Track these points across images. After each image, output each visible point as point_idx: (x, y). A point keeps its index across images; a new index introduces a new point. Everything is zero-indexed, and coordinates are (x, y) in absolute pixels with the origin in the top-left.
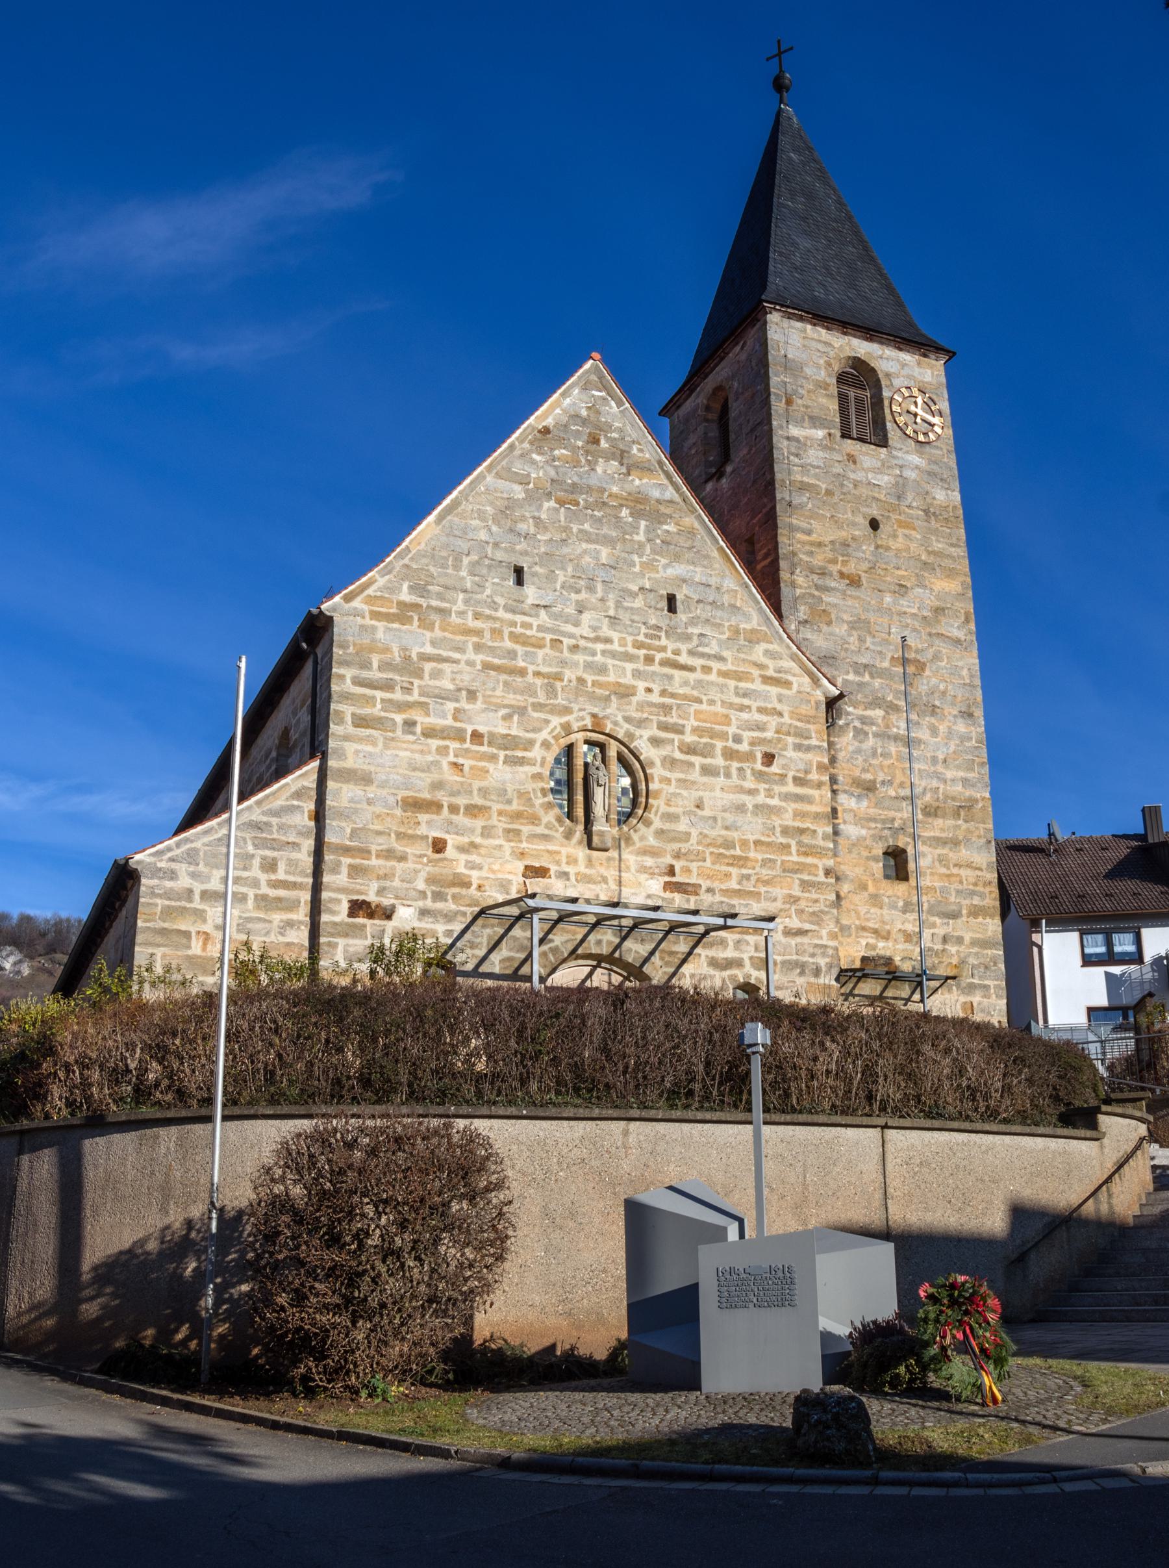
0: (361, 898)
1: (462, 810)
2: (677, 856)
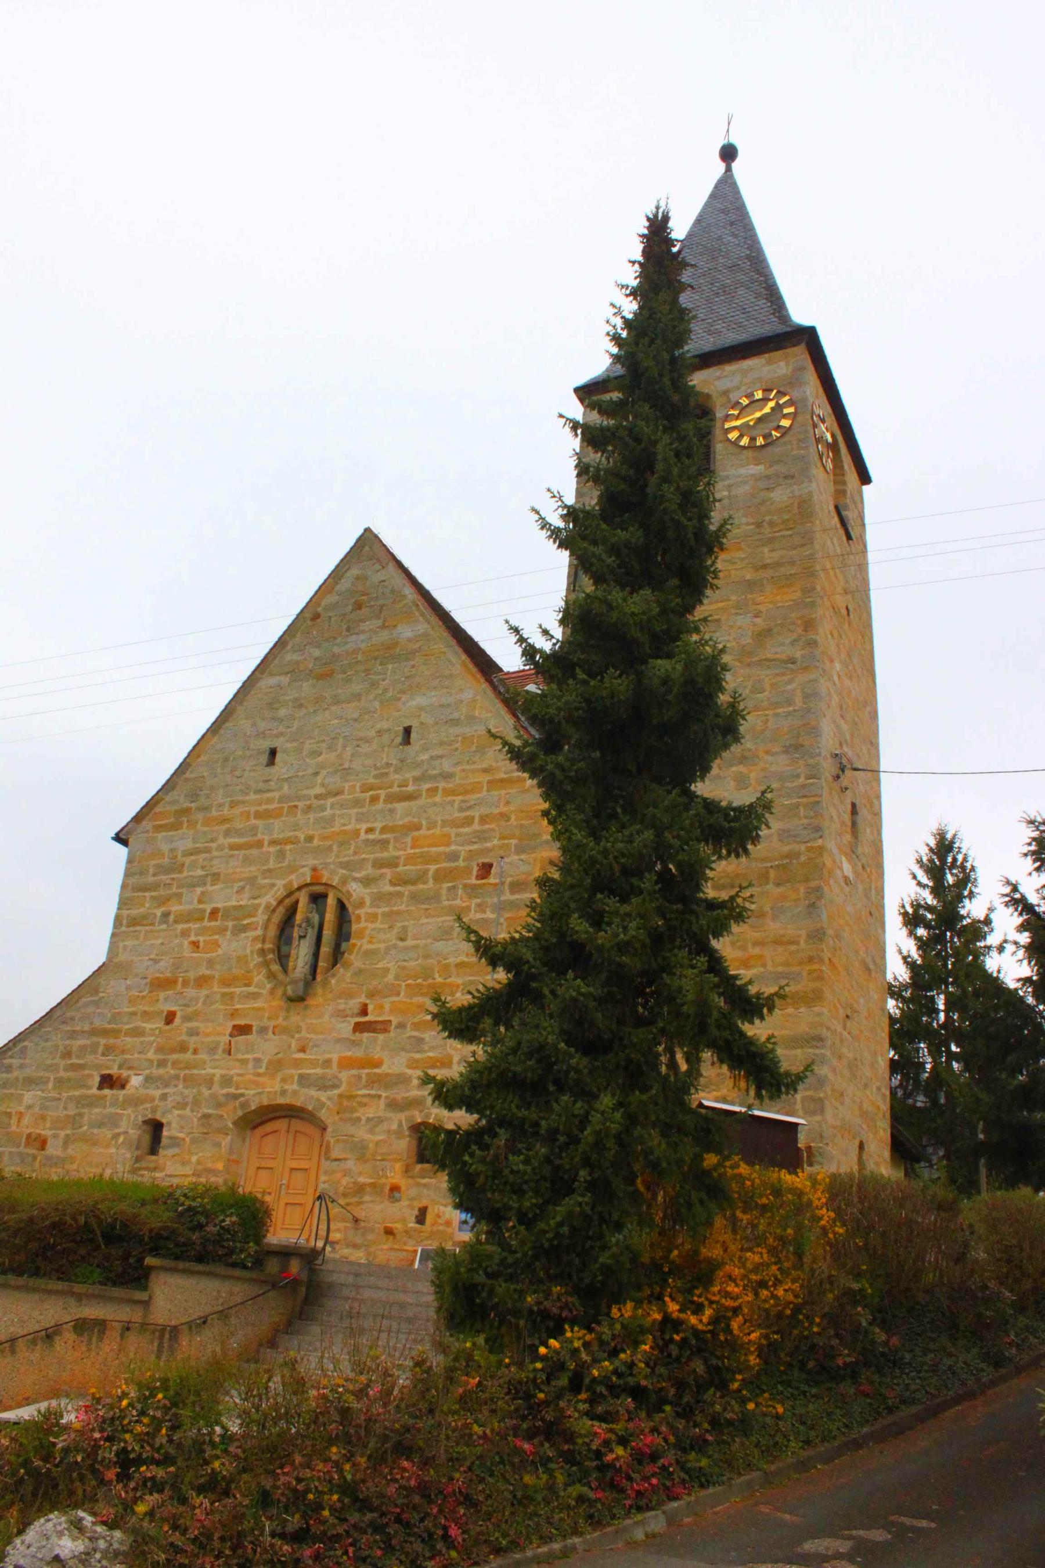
0: (107, 1072)
1: (192, 983)
2: (371, 995)
